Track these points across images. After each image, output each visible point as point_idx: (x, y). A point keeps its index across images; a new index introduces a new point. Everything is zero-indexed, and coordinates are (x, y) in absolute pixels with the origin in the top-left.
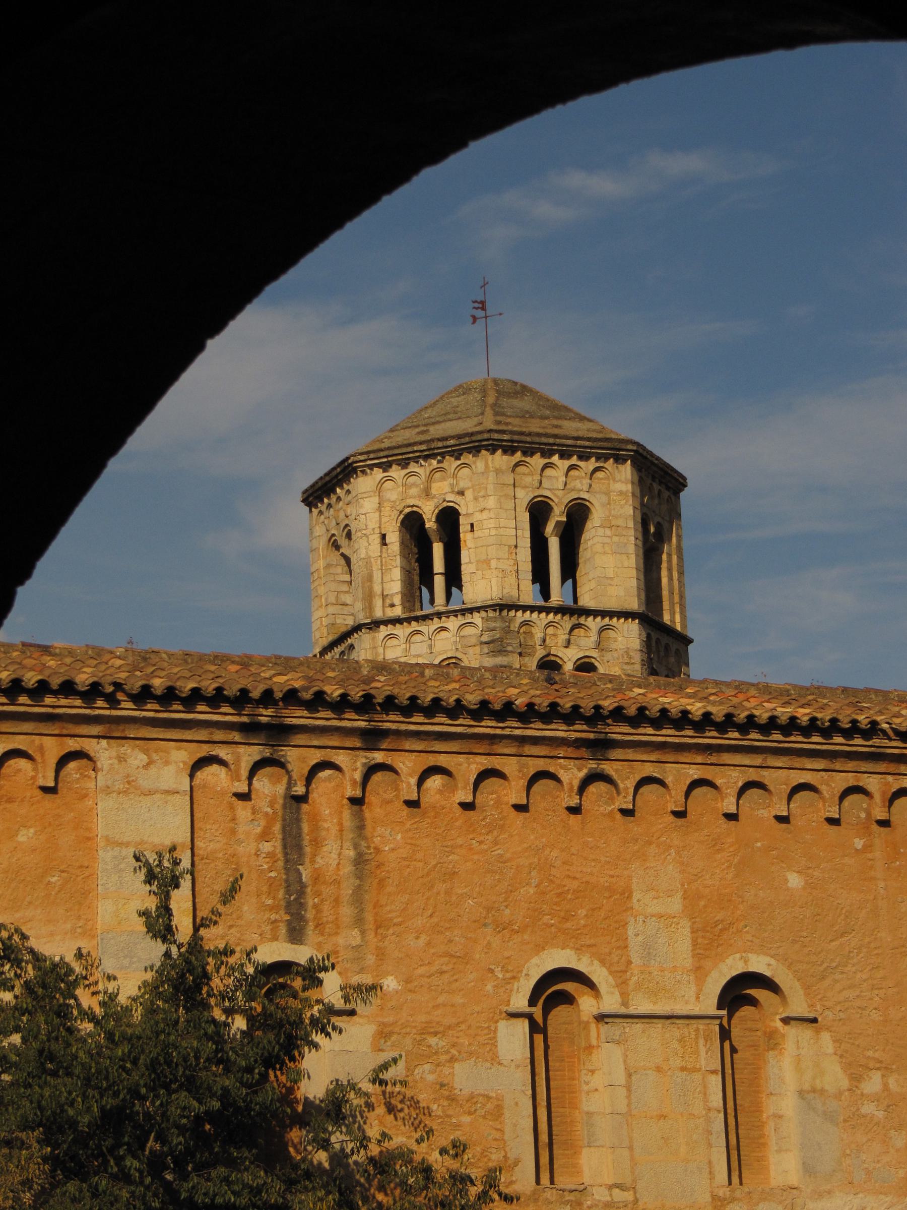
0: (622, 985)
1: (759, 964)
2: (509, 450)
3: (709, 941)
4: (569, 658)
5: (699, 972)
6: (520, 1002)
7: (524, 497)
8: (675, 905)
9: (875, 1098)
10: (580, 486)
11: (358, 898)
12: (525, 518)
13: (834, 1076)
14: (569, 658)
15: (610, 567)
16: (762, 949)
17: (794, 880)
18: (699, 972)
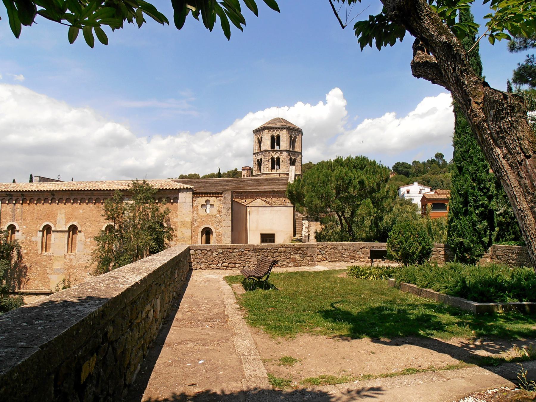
0: (55, 226)
1: (75, 223)
2: (268, 129)
3: (68, 220)
4: (275, 157)
5: (66, 224)
6: (41, 229)
7: (270, 135)
8: (64, 215)
9: (89, 242)
10: (278, 133)
11: (21, 216)
12: (270, 138)
13: (84, 239)
14: (275, 157)
15: (284, 144)
16: (74, 221)
17: (81, 211)
18: (66, 224)
